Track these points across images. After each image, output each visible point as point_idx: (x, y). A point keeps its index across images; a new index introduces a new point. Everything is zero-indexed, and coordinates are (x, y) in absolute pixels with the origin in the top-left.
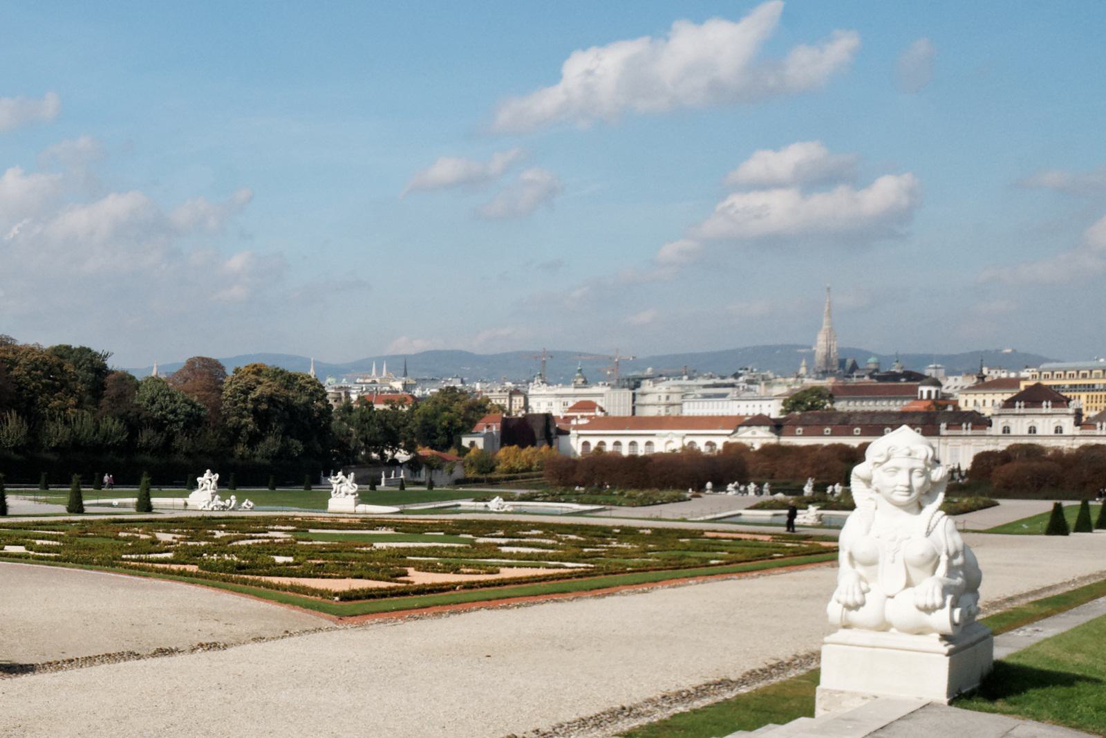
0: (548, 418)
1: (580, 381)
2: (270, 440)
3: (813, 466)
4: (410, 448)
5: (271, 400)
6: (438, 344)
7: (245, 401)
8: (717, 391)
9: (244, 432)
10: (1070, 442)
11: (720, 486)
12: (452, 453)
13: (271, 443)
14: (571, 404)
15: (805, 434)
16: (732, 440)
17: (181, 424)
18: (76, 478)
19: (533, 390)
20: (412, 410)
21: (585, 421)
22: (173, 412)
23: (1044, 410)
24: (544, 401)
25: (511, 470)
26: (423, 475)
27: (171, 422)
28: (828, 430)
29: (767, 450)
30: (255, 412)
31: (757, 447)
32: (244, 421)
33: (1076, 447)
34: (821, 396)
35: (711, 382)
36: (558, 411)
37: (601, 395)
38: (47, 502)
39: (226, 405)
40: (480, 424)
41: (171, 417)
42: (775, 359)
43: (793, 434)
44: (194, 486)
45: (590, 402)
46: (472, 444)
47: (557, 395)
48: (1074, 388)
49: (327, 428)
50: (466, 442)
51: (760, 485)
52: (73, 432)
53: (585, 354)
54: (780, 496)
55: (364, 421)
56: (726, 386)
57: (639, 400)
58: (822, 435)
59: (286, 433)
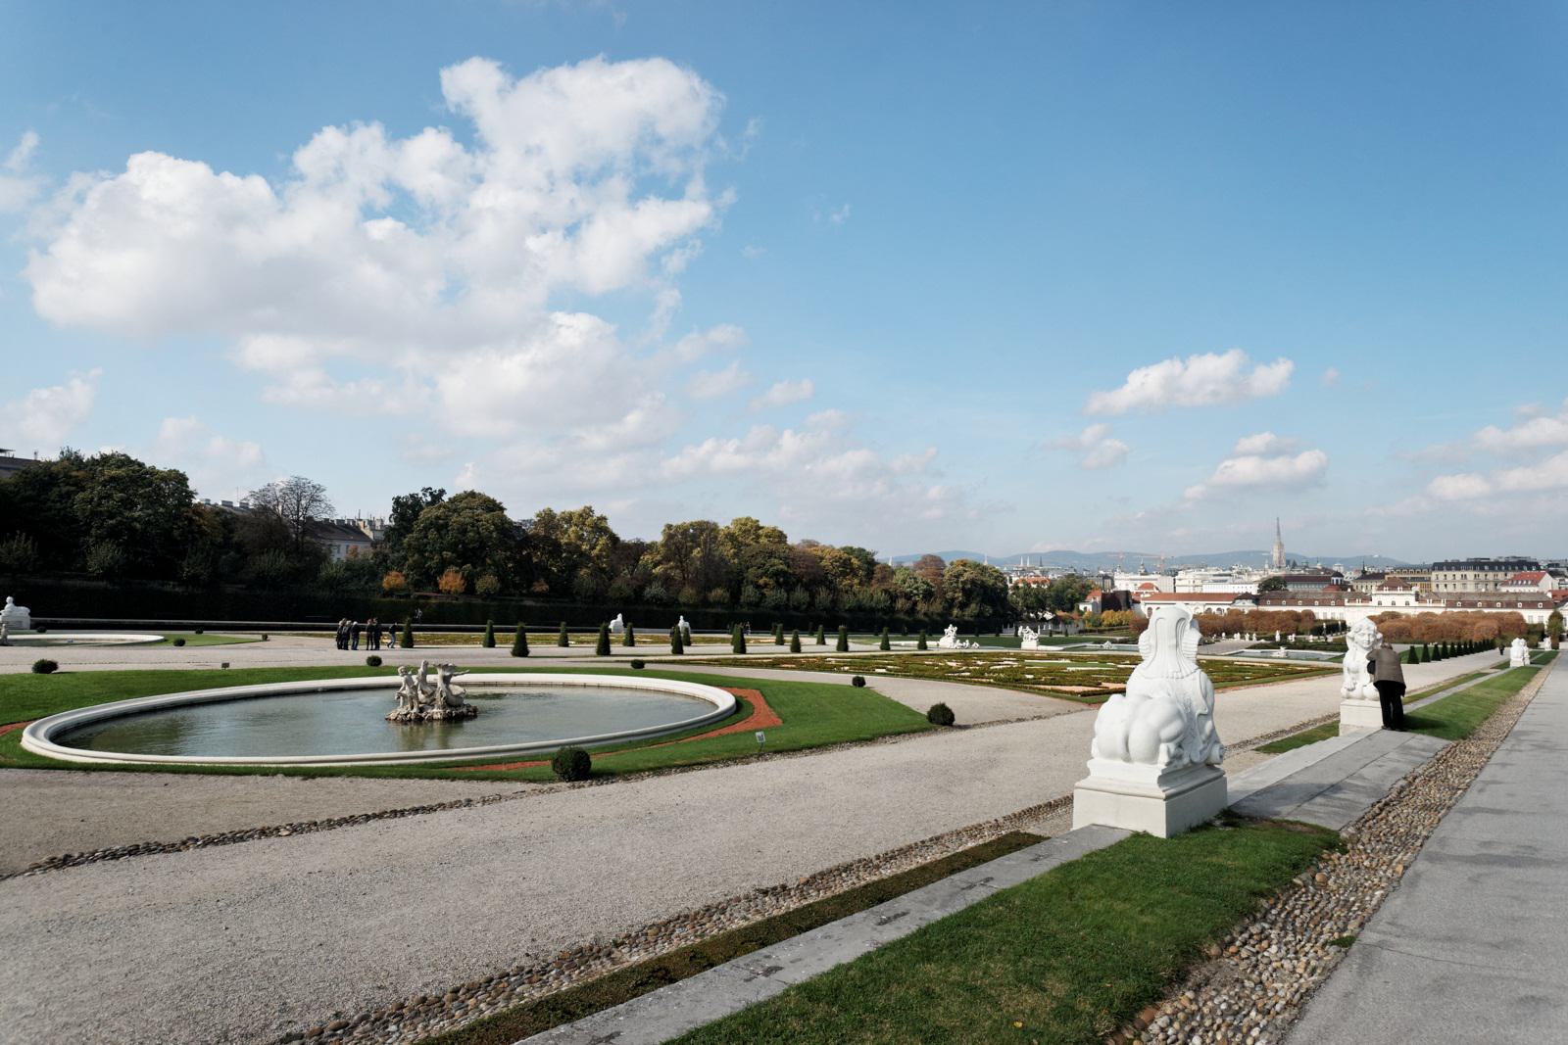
0: (1127, 593)
1: (1143, 571)
2: (973, 606)
3: (1278, 623)
4: (1053, 611)
5: (973, 582)
6: (1060, 547)
7: (957, 582)
8: (1221, 579)
9: (956, 601)
10: (1414, 610)
11: (1229, 635)
12: (1074, 614)
13: (973, 608)
14: (1139, 585)
15: (1272, 605)
16: (1231, 608)
17: (921, 596)
18: (885, 629)
19: (1117, 576)
20: (1049, 588)
21: (1148, 595)
22: (917, 589)
23: (1399, 592)
24: (1123, 583)
25: (1110, 625)
26: (1061, 627)
27: (915, 595)
28: (1284, 602)
29: (1252, 614)
30: (963, 589)
31: (1246, 612)
32: (956, 595)
33: (1417, 613)
34: (1279, 582)
35: (1217, 573)
36: (1132, 589)
37: (1156, 580)
38: (860, 643)
39: (946, 585)
40: (1088, 598)
41: (915, 592)
42: (1255, 559)
43: (1266, 605)
44: (943, 633)
45: (1150, 584)
46: (1085, 608)
47: (1131, 579)
48: (1413, 579)
49: (1005, 598)
50: (1082, 607)
51: (1251, 634)
52: (858, 601)
53: (1146, 555)
54: (1263, 641)
55: (1026, 594)
56: (1226, 575)
57: (1178, 582)
58: (1281, 605)
59: (983, 601)
